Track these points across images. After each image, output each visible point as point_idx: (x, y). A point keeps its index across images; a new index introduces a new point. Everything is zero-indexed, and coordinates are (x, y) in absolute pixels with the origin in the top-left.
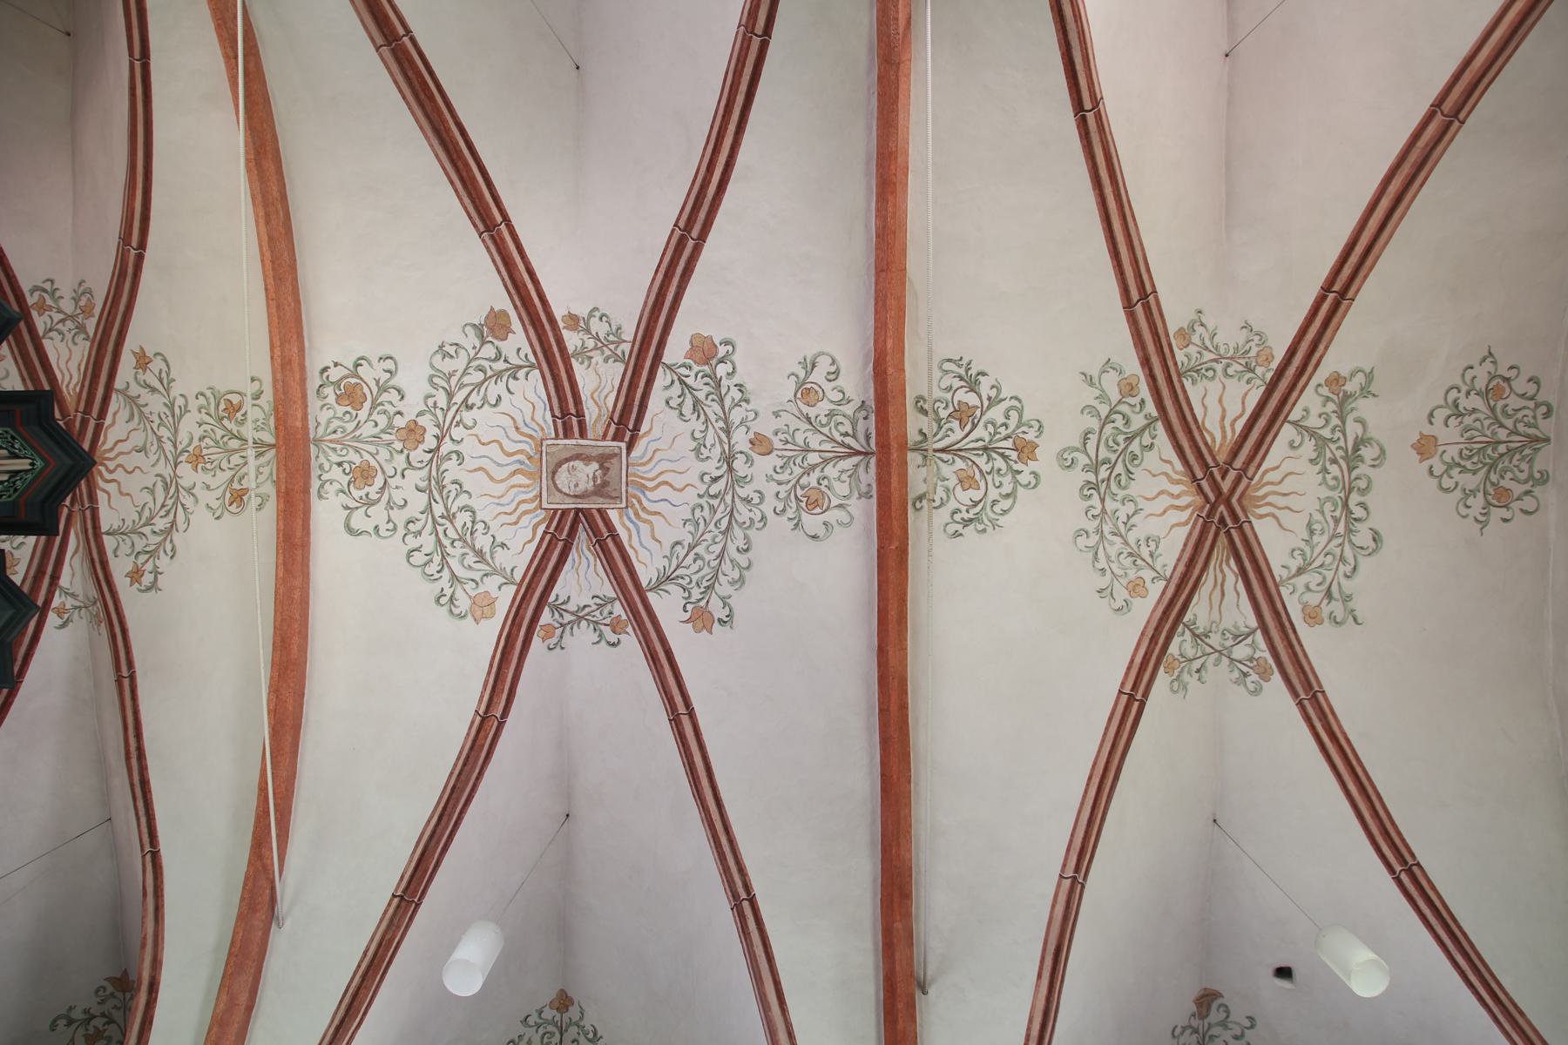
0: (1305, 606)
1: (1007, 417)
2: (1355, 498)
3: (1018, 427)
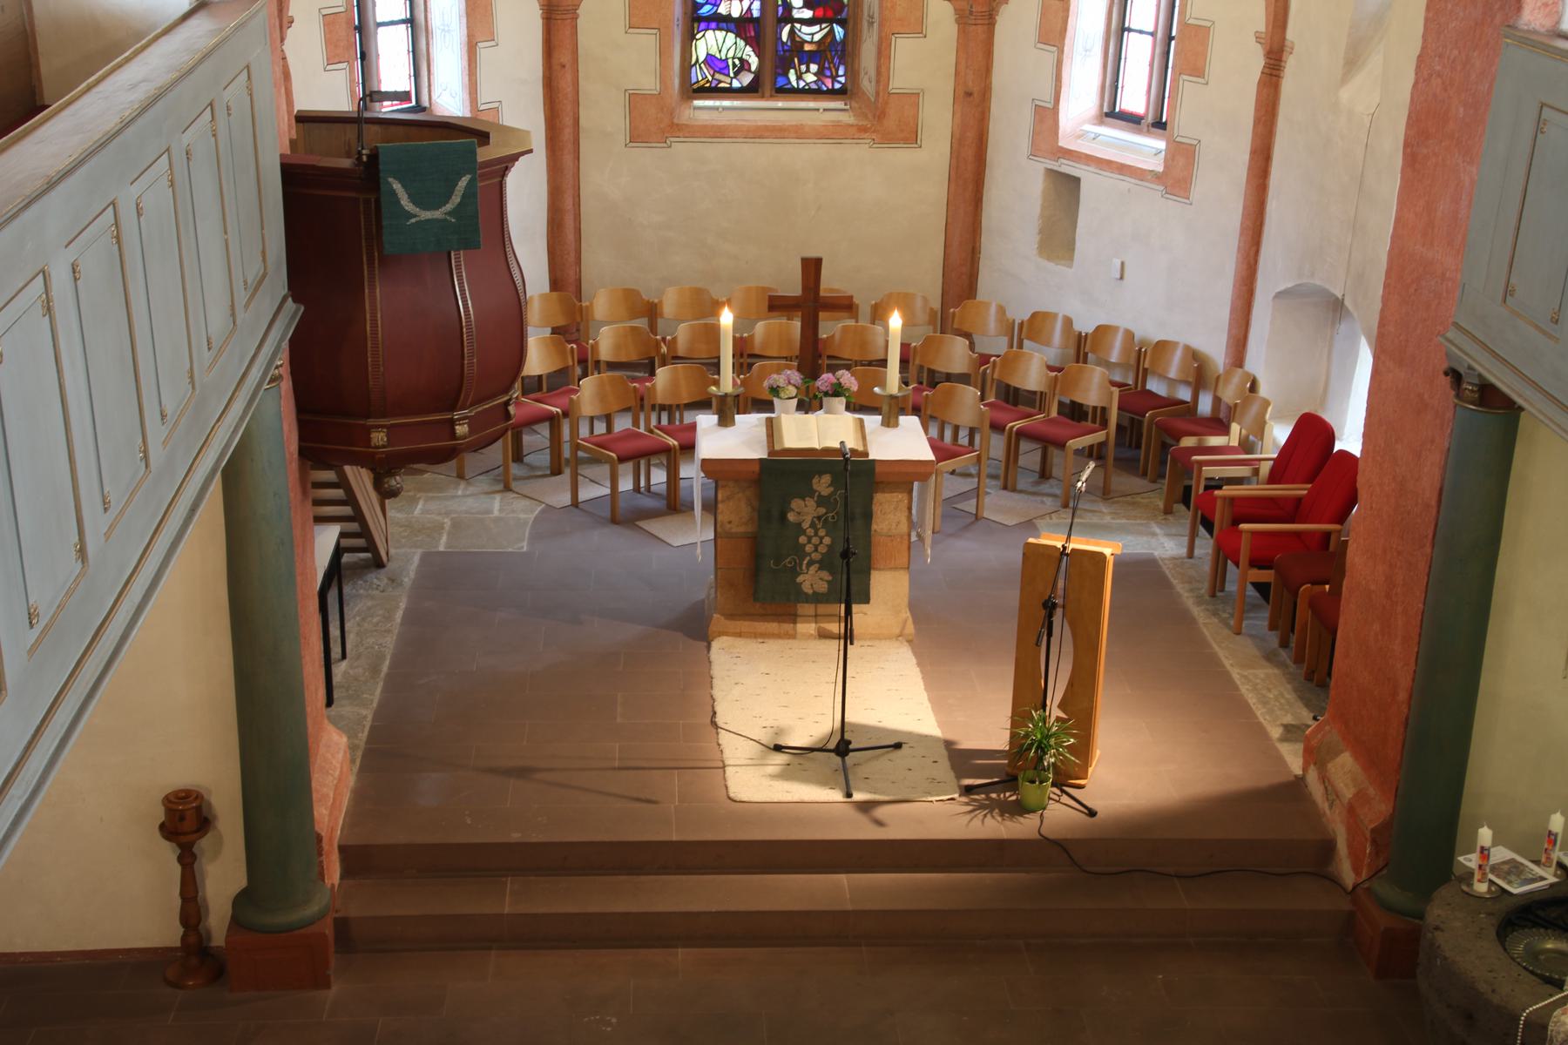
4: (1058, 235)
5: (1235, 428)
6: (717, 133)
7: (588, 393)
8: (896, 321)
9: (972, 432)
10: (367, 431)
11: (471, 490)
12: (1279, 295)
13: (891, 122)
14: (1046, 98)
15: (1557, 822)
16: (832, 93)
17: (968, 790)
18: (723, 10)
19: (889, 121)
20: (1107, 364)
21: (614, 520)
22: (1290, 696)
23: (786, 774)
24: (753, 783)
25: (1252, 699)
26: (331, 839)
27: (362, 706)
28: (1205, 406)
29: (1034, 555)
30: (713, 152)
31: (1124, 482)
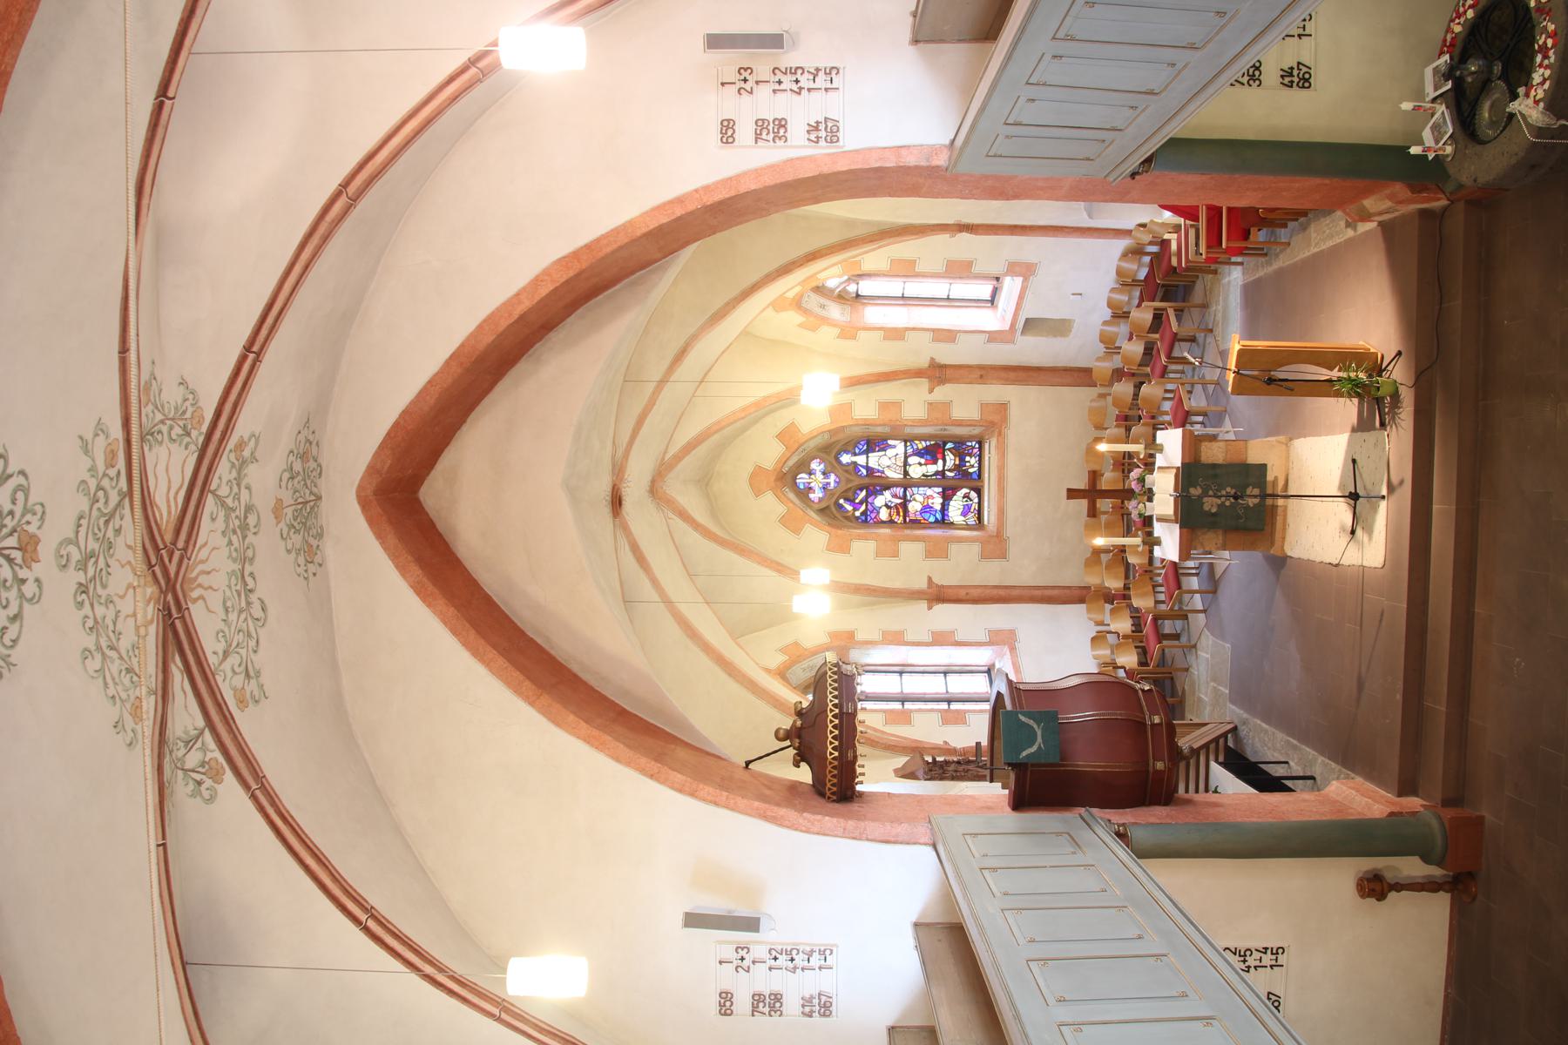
0: (235, 689)
1: (14, 502)
2: (248, 569)
3: (23, 516)
4: (1059, 327)
5: (1166, 236)
6: (1001, 513)
7: (1143, 602)
8: (1103, 447)
9: (1167, 391)
10: (1157, 772)
12: (1090, 216)
13: (996, 418)
14: (984, 337)
15: (1407, 106)
16: (980, 449)
17: (1383, 424)
18: (938, 507)
19: (996, 420)
20: (1129, 302)
21: (1215, 592)
22: (1328, 220)
23: (1369, 531)
24: (1374, 550)
25: (1330, 243)
26: (1393, 804)
27: (1321, 765)
28: (1154, 249)
29: (1239, 389)
30: (1011, 513)
31: (1197, 296)
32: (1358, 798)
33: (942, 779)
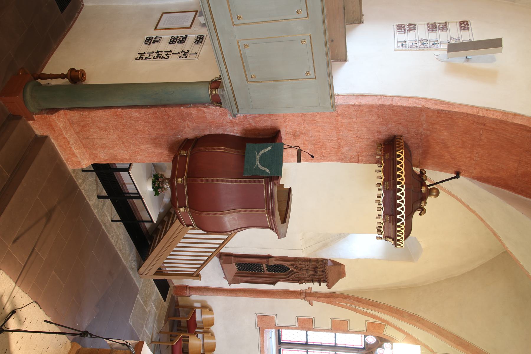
11: (155, 333)
32: (71, 141)
33: (317, 260)
